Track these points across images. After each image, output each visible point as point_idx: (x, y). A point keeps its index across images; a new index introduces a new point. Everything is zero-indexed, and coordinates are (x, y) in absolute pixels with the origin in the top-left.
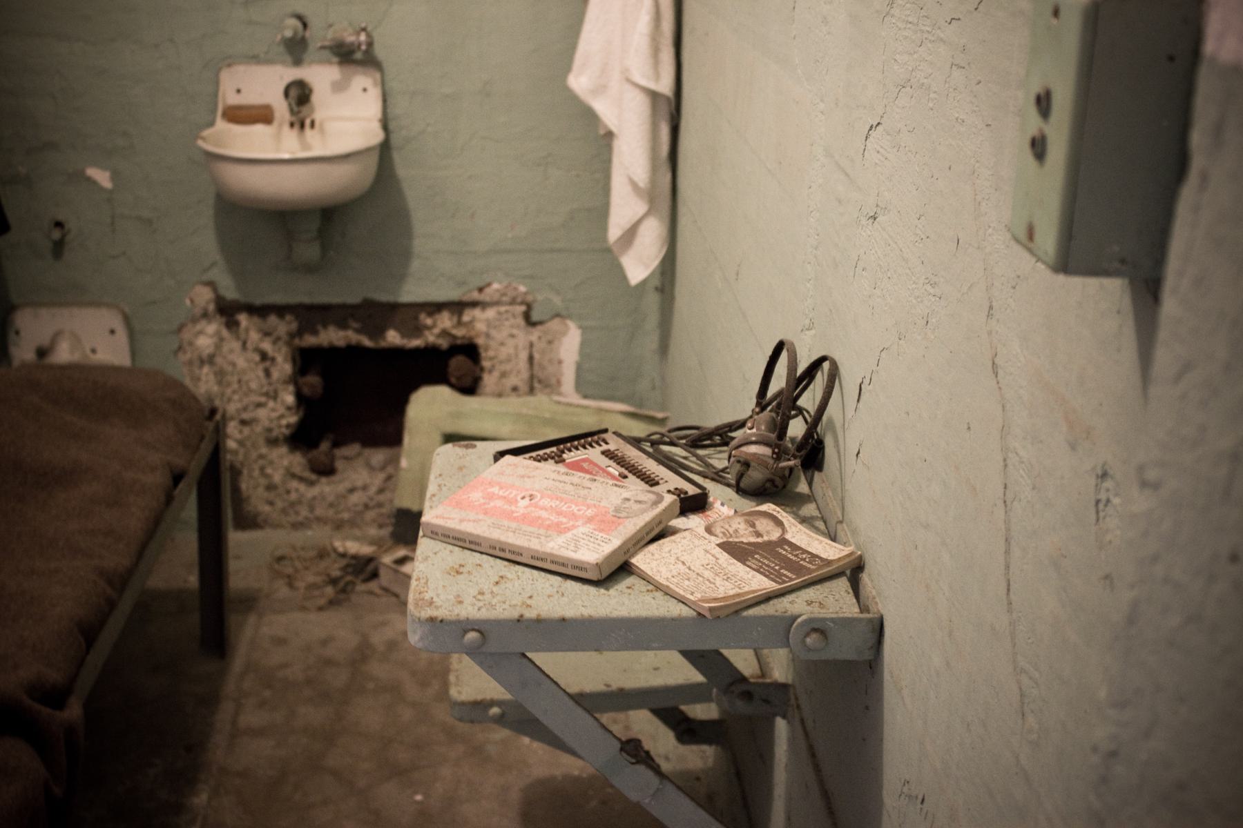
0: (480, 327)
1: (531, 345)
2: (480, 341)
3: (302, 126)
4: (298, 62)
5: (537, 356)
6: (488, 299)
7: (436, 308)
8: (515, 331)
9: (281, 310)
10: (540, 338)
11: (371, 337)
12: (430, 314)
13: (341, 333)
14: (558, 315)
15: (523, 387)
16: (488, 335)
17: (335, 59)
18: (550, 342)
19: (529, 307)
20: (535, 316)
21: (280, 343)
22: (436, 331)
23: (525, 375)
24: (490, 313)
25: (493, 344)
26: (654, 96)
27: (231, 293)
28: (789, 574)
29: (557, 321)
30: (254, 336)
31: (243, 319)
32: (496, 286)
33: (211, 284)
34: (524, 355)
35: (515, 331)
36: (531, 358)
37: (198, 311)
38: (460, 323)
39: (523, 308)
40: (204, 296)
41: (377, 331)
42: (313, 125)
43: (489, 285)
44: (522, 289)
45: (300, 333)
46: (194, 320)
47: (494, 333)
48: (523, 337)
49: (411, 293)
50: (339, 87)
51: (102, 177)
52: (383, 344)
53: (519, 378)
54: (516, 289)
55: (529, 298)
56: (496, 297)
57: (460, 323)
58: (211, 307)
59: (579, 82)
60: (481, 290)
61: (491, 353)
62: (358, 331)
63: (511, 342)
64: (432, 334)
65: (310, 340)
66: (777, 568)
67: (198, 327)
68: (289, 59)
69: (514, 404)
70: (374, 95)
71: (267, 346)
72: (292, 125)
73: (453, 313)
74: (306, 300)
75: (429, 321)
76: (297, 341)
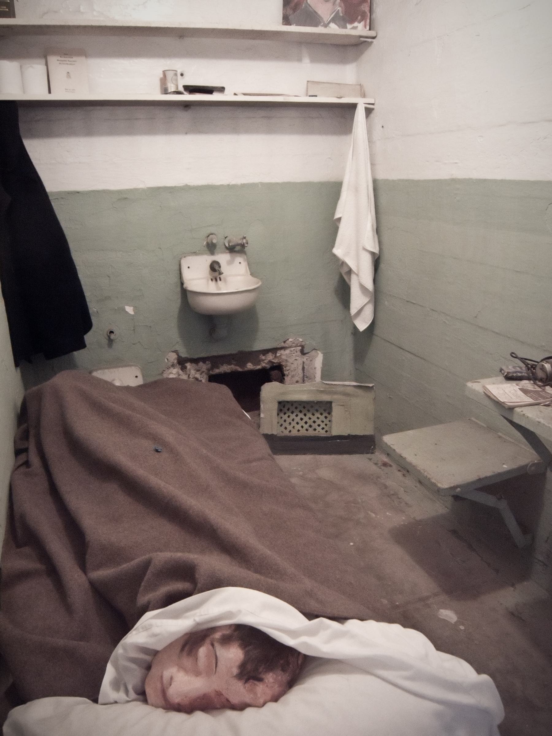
0: (284, 357)
1: (304, 363)
2: (283, 364)
3: (216, 280)
4: (212, 253)
5: (306, 367)
6: (287, 346)
7: (265, 352)
8: (297, 358)
9: (204, 360)
10: (307, 359)
11: (241, 368)
12: (264, 355)
13: (229, 367)
14: (314, 349)
15: (300, 380)
16: (287, 361)
17: (228, 251)
18: (311, 361)
19: (303, 347)
20: (305, 352)
21: (204, 374)
22: (266, 361)
23: (301, 375)
24: (287, 351)
25: (289, 364)
26: (373, 254)
27: (184, 355)
28: (541, 399)
29: (313, 352)
30: (193, 372)
31: (188, 365)
32: (290, 340)
33: (176, 352)
34: (301, 367)
35: (297, 358)
36: (303, 368)
37: (170, 364)
38: (276, 357)
39: (300, 348)
40: (173, 357)
41: (244, 364)
42: (220, 280)
43: (288, 339)
44: (301, 340)
45: (212, 369)
46: (168, 368)
47: (289, 360)
48: (301, 359)
49: (258, 346)
50: (230, 263)
51: (130, 310)
52: (246, 369)
53: (299, 377)
54: (298, 340)
55: (303, 343)
56: (290, 344)
57: (276, 357)
58: (176, 362)
59: (338, 251)
60: (284, 342)
61: (288, 368)
62: (236, 365)
63: (296, 362)
64: (264, 363)
65: (217, 371)
66: (537, 397)
67: (170, 371)
68: (208, 252)
69: (298, 387)
70: (244, 265)
71: (198, 376)
72: (212, 280)
73: (273, 354)
74: (215, 354)
75: (263, 358)
76: (211, 372)
